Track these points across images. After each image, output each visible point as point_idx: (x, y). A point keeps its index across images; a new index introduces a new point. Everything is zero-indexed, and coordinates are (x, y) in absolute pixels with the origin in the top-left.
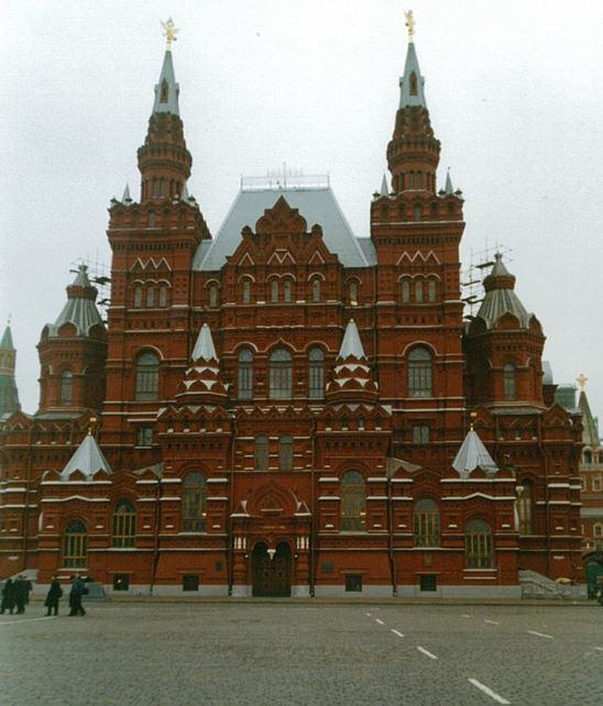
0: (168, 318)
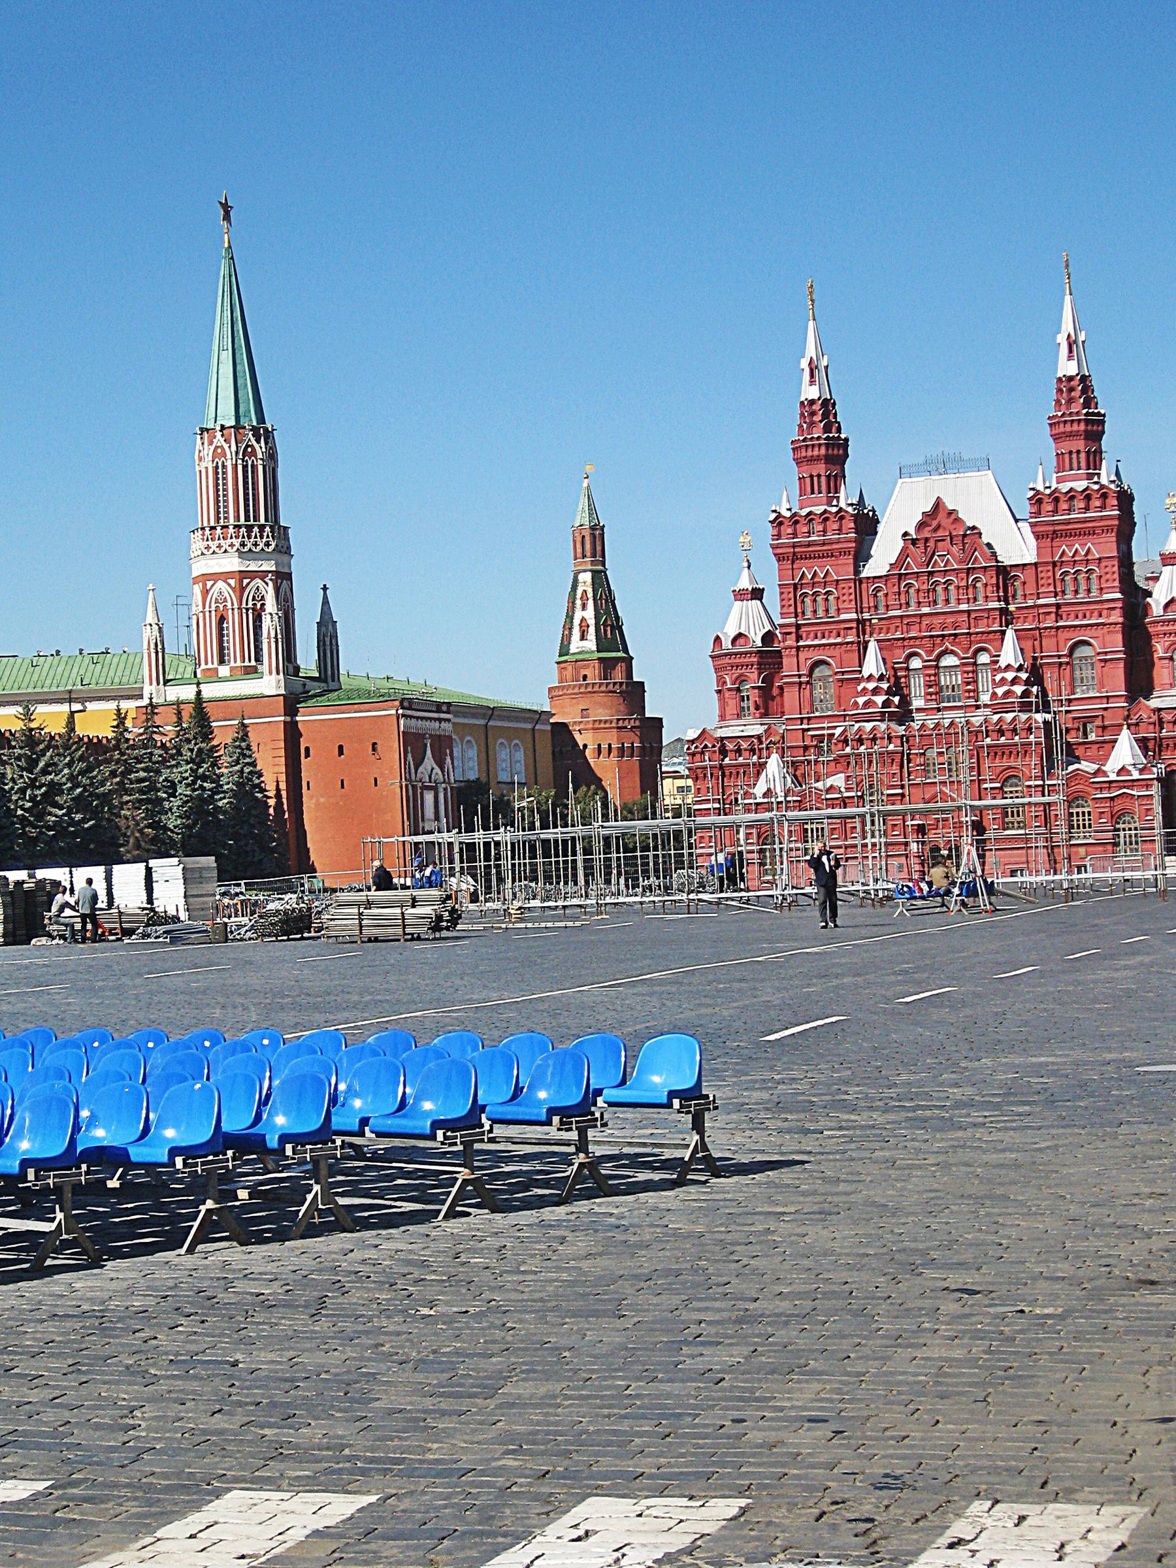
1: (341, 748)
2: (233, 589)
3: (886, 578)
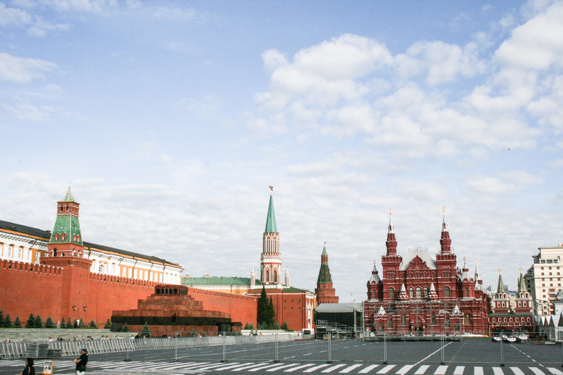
0: (395, 281)
3: (405, 271)
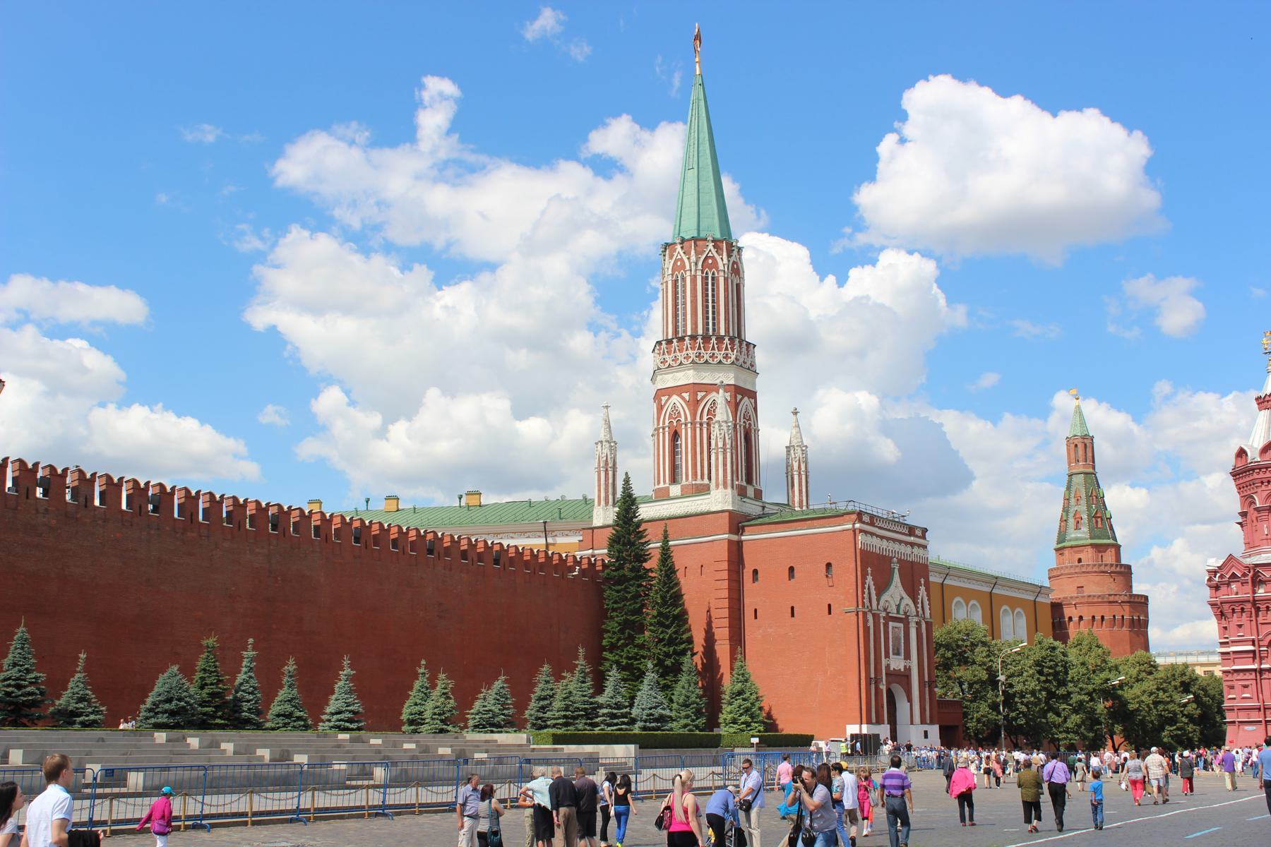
1: (791, 569)
2: (687, 403)
